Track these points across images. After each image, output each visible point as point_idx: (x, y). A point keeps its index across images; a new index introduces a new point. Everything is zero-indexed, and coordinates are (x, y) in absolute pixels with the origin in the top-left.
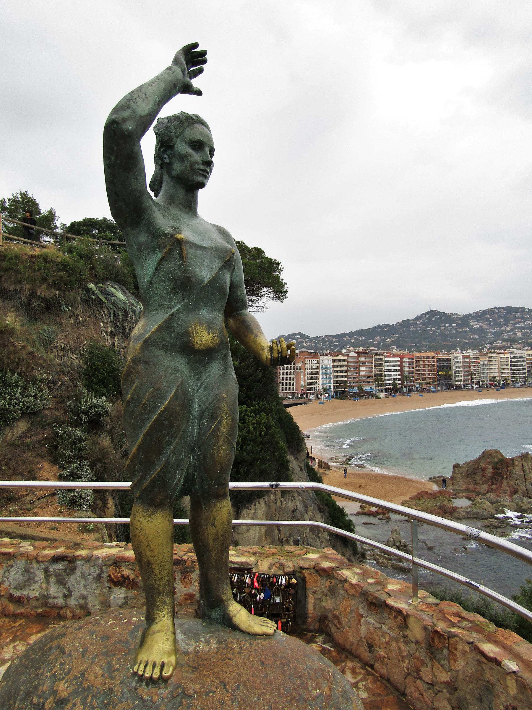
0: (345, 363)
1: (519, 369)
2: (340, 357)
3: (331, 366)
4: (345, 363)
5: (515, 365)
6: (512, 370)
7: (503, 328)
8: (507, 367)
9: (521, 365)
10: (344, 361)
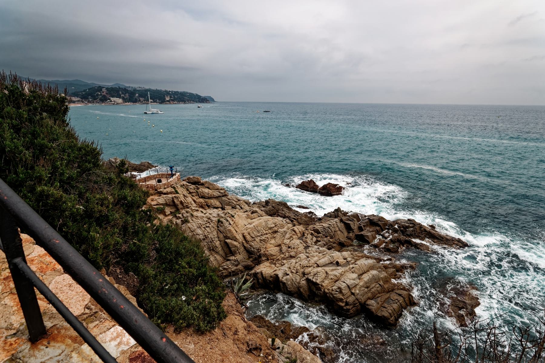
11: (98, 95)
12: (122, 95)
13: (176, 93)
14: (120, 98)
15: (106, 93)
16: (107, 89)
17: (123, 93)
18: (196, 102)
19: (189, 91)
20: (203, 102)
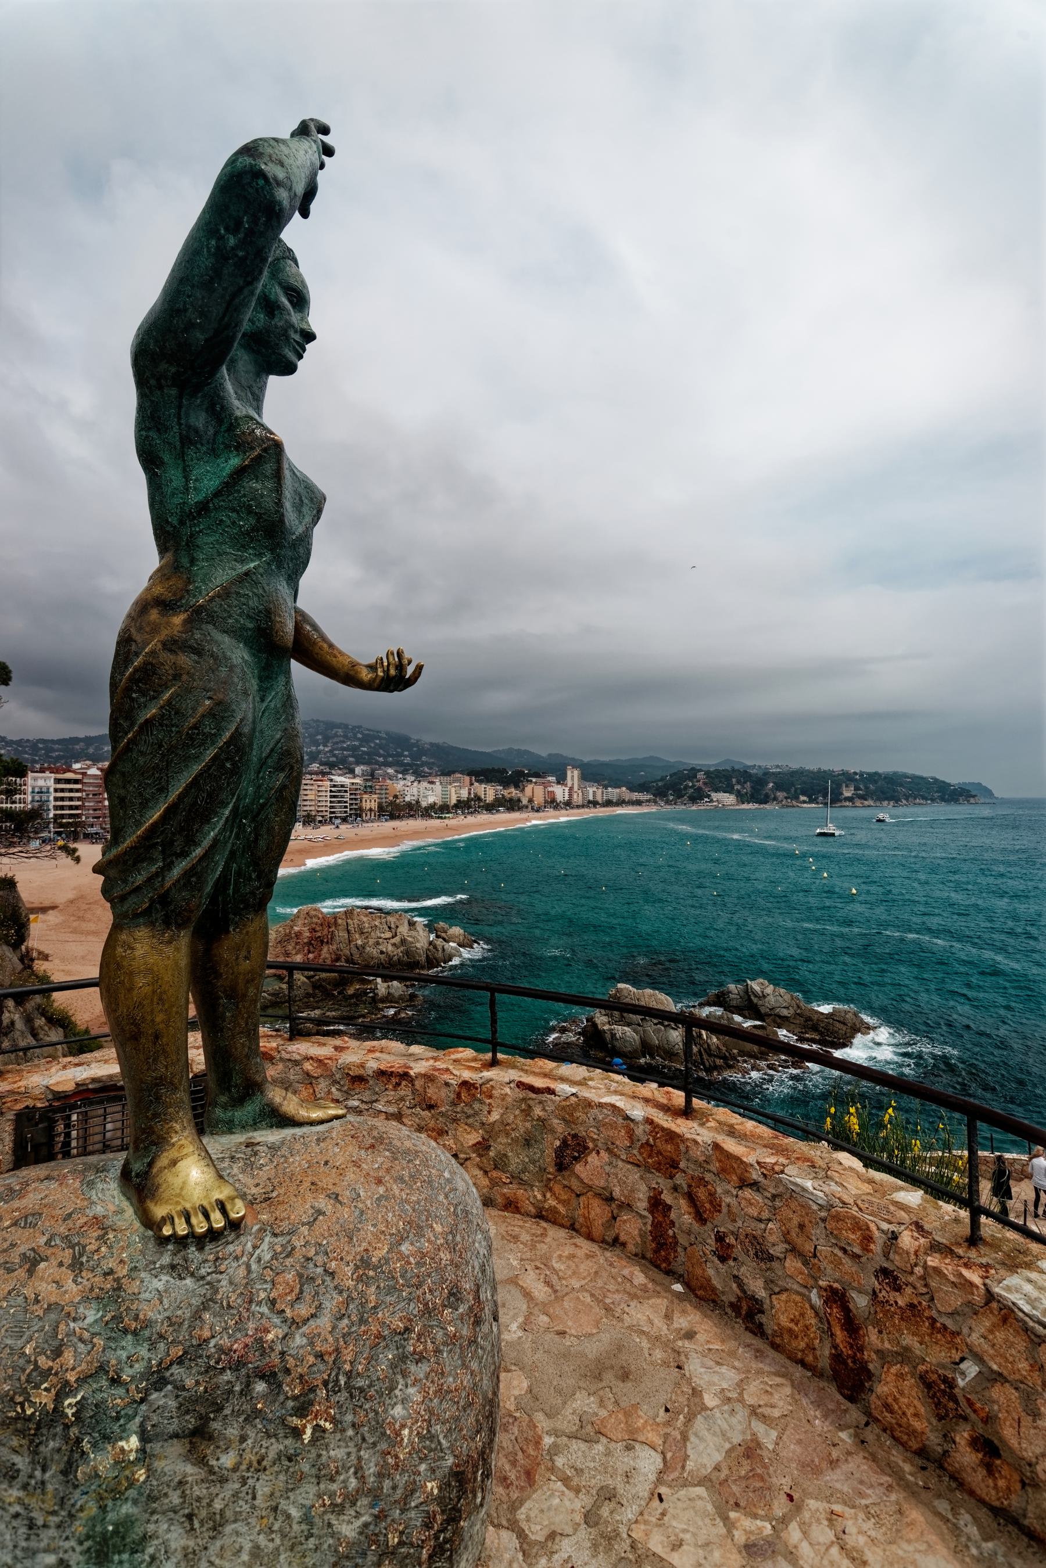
0: (79, 786)
1: (339, 802)
2: (69, 775)
3: (52, 790)
4: (79, 786)
5: (334, 797)
6: (331, 802)
7: (321, 747)
8: (326, 799)
9: (342, 797)
10: (76, 782)
11: (686, 787)
12: (739, 787)
13: (873, 777)
14: (730, 793)
15: (705, 784)
16: (708, 773)
17: (738, 782)
19: (910, 771)
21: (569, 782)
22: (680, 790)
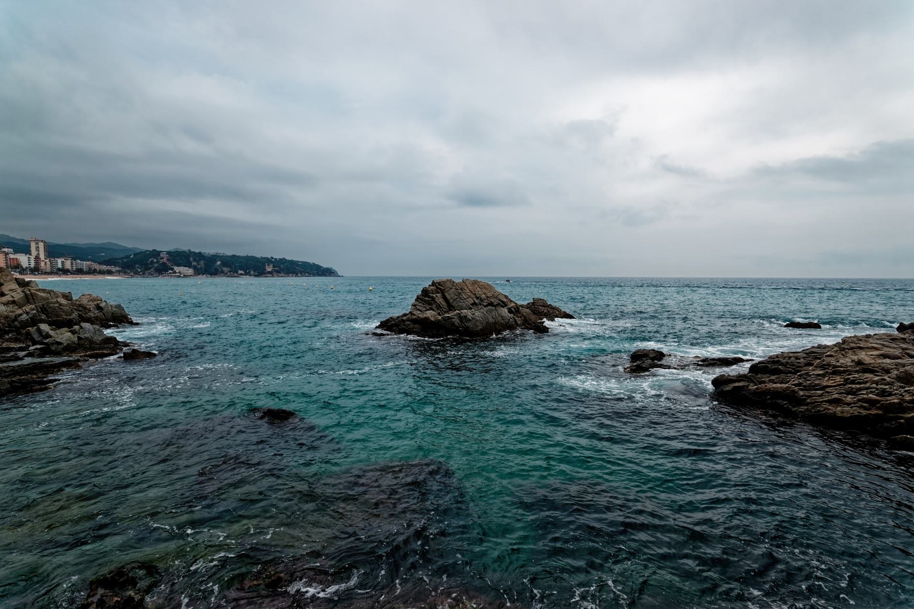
11: (152, 262)
15: (168, 260)
16: (169, 253)
18: (314, 275)
20: (325, 275)
21: (34, 253)
22: (146, 264)
